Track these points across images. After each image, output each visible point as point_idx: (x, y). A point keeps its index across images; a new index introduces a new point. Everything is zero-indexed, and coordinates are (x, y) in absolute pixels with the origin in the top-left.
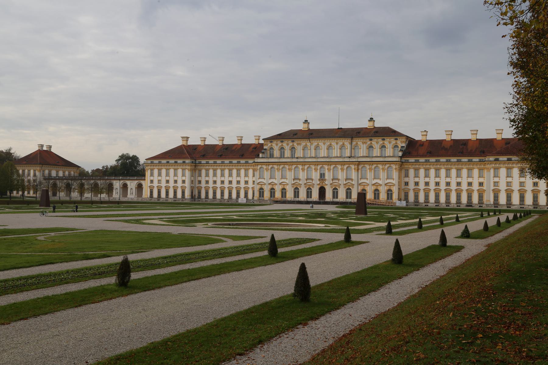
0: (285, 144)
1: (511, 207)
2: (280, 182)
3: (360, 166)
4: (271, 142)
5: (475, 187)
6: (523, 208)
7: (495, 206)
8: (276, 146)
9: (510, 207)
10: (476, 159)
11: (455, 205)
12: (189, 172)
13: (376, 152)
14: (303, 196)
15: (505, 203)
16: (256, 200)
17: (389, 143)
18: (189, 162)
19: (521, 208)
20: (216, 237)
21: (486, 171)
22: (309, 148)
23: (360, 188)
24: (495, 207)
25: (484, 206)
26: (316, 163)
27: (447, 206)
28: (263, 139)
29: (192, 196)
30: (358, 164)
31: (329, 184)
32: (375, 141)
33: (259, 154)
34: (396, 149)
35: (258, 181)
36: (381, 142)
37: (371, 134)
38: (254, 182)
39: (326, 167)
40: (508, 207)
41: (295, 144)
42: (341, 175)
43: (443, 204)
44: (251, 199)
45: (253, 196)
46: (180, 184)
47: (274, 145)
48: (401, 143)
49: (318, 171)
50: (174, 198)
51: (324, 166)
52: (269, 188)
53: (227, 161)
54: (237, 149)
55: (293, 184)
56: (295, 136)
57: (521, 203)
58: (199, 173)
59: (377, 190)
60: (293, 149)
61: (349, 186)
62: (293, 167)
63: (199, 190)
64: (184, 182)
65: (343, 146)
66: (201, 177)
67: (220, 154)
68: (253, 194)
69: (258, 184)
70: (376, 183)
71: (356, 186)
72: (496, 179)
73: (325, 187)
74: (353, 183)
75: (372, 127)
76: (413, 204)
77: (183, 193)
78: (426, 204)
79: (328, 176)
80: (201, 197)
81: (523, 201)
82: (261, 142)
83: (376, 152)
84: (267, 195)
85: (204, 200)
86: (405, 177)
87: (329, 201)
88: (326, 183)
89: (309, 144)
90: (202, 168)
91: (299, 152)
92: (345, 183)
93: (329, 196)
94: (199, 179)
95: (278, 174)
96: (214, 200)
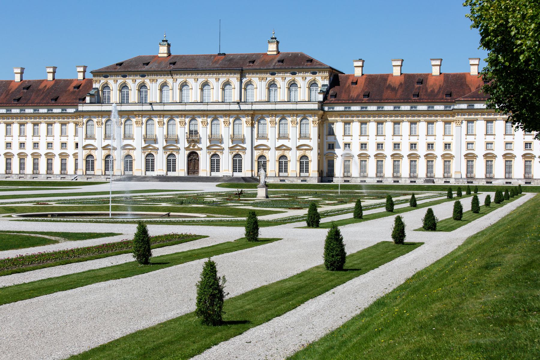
1: (493, 183)
3: (255, 117)
5: (439, 150)
6: (510, 183)
7: (469, 180)
8: (114, 84)
9: (491, 183)
11: (407, 180)
14: (160, 168)
15: (484, 177)
16: (80, 175)
19: (507, 183)
20: (40, 236)
21: (453, 125)
22: (170, 88)
23: (257, 153)
24: (468, 182)
26: (183, 114)
27: (395, 182)
28: (91, 72)
31: (204, 149)
32: (279, 77)
33: (85, 98)
34: (314, 88)
35: (84, 144)
36: (289, 77)
37: (273, 64)
38: (77, 144)
40: (487, 183)
43: (388, 179)
44: (73, 173)
45: (76, 169)
48: (322, 80)
49: (187, 126)
52: (103, 154)
54: (47, 88)
56: (146, 68)
57: (507, 176)
59: (283, 157)
61: (237, 151)
65: (227, 84)
67: (18, 97)
68: (76, 165)
69: (84, 148)
70: (283, 145)
71: (249, 151)
72: (470, 139)
73: (198, 152)
75: (275, 53)
76: (340, 179)
81: (510, 172)
82: (89, 76)
83: (281, 94)
88: (200, 146)
92: (231, 145)
96: (7, 176)
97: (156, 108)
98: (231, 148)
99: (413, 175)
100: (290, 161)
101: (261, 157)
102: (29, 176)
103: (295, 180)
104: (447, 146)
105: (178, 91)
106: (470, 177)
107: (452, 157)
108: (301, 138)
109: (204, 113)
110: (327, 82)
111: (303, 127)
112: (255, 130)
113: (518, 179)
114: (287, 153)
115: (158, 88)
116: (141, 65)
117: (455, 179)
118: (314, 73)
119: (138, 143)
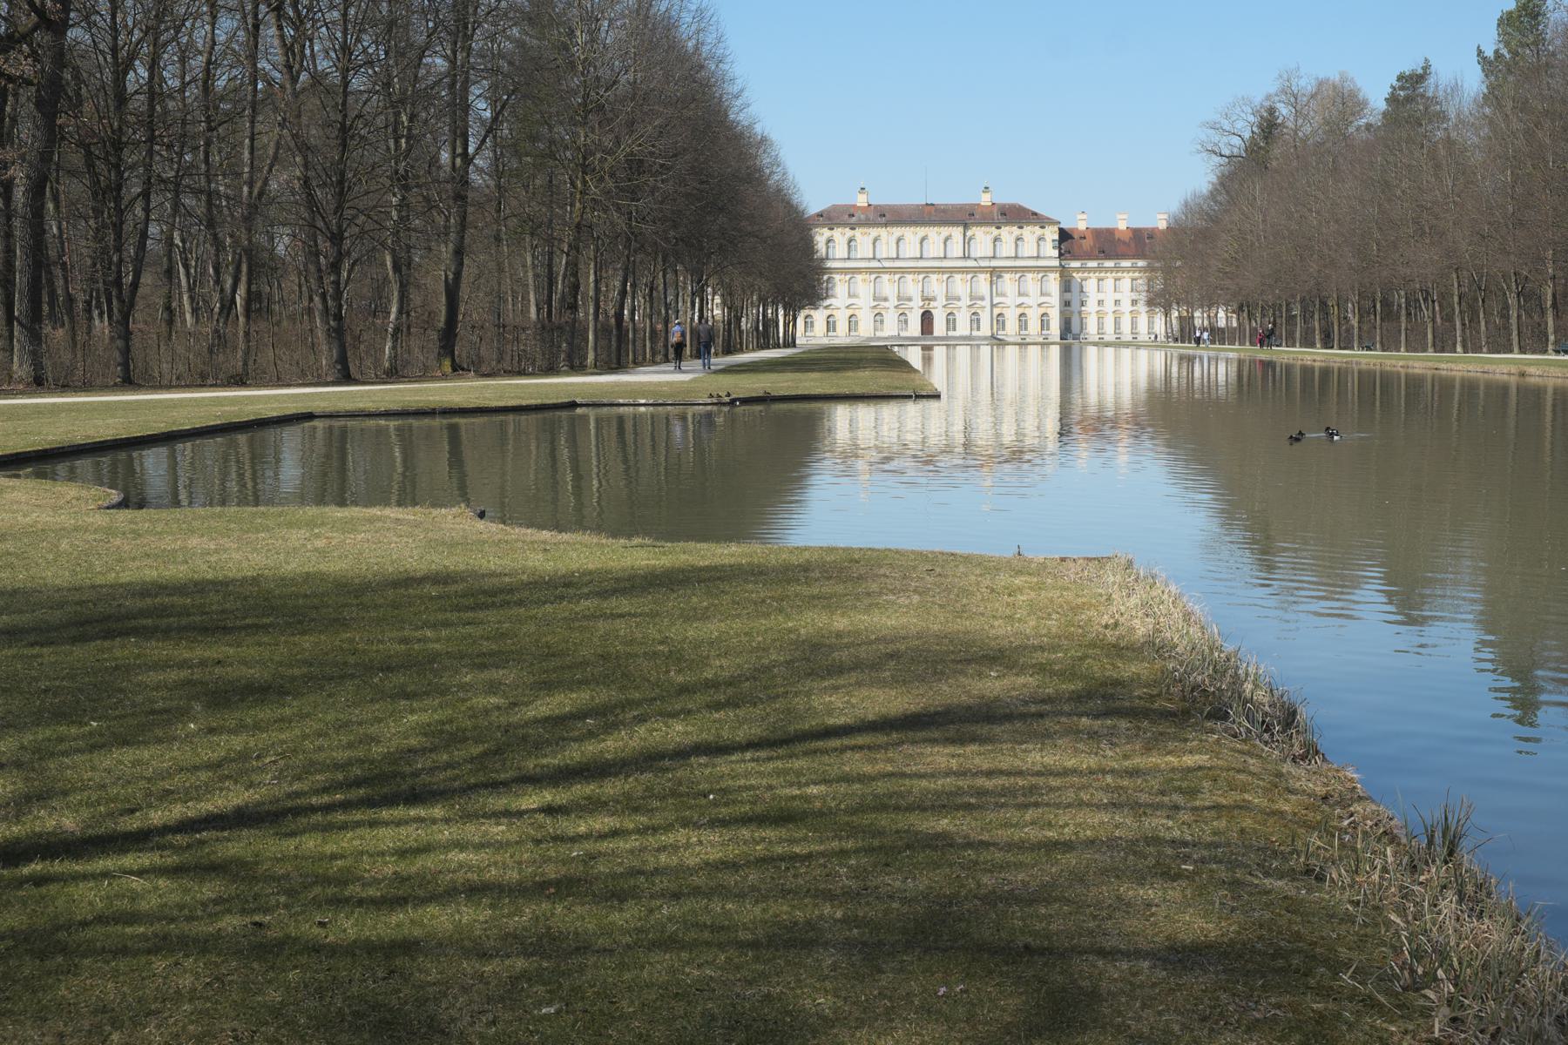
13: (1007, 249)
17: (1030, 233)
23: (996, 311)
48: (1051, 234)
55: (875, 307)
73: (932, 311)
86: (1066, 291)
92: (969, 303)
97: (887, 264)
98: (970, 306)
101: (999, 315)
105: (894, 246)
108: (1042, 294)
110: (1056, 237)
111: (1044, 283)
112: (994, 286)
114: (1027, 311)
115: (871, 242)
118: (1042, 227)
119: (864, 301)
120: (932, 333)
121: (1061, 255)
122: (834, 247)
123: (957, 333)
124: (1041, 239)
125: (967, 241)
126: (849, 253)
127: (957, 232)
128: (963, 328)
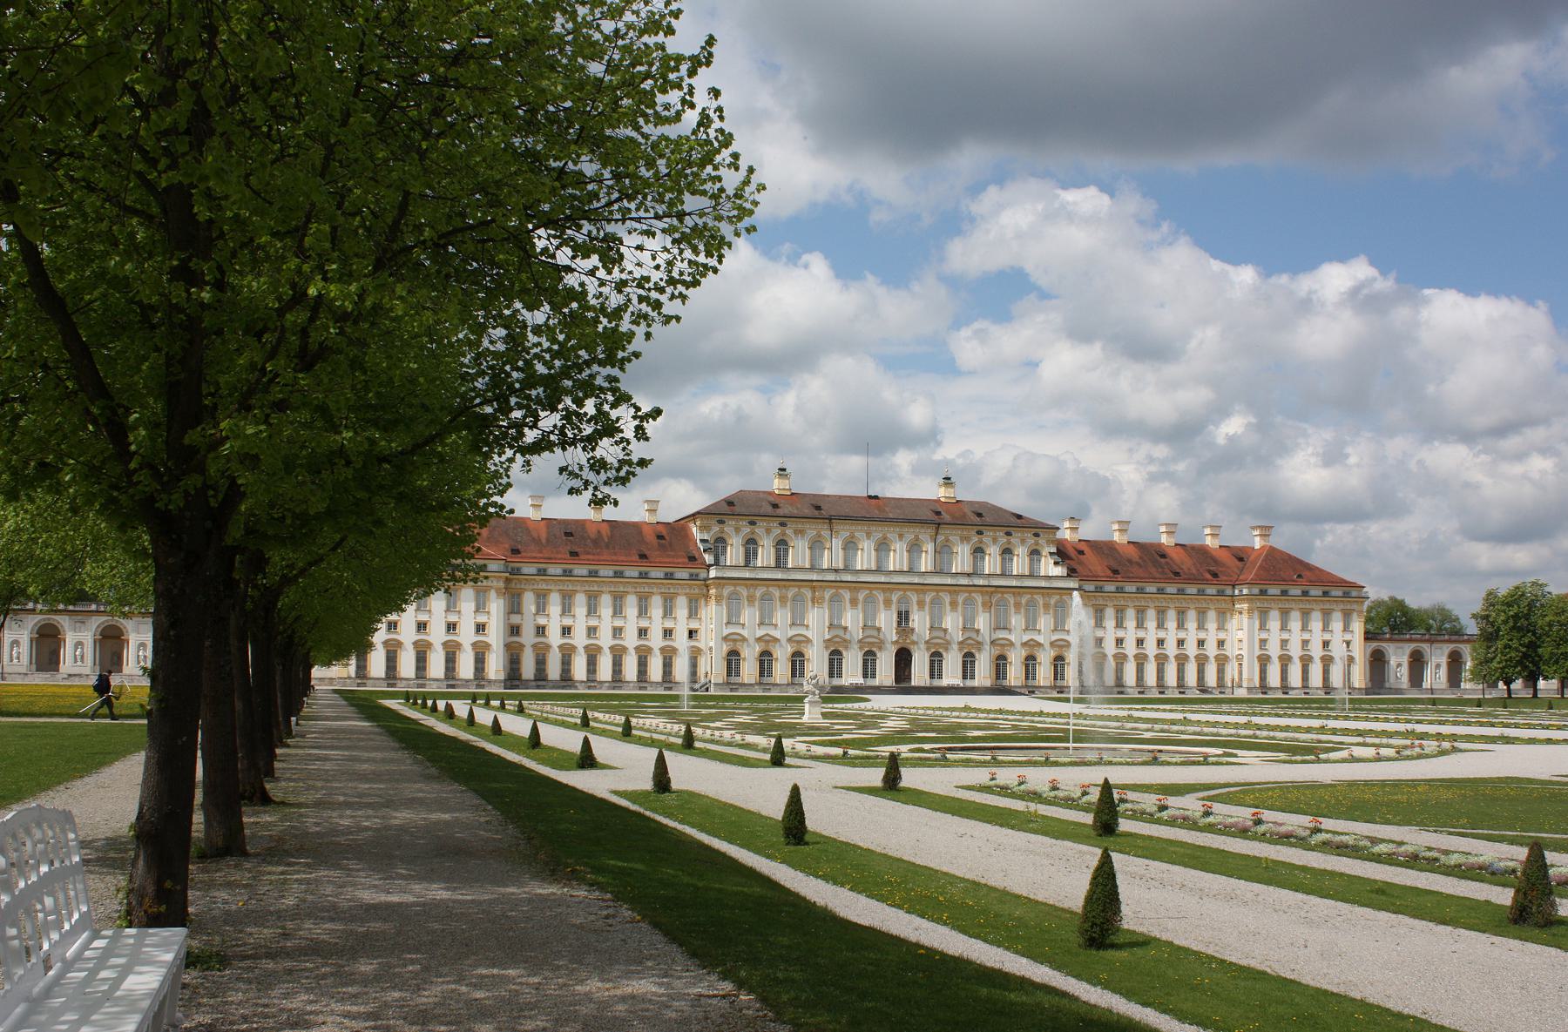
0: (759, 531)
2: (789, 636)
4: (721, 522)
5: (1211, 650)
6: (1307, 693)
10: (1211, 590)
12: (501, 602)
13: (991, 564)
18: (502, 568)
25: (1227, 691)
26: (888, 587)
29: (513, 676)
30: (992, 593)
39: (914, 598)
41: (789, 532)
42: (952, 622)
43: (1154, 690)
46: (467, 635)
47: (728, 529)
50: (447, 677)
51: (909, 593)
53: (606, 571)
56: (780, 512)
58: (513, 602)
60: (781, 546)
62: (827, 595)
63: (512, 655)
64: (480, 628)
66: (522, 614)
69: (725, 639)
70: (1032, 640)
74: (980, 639)
77: (480, 661)
78: (1119, 689)
79: (919, 622)
80: (521, 675)
84: (749, 671)
85: (534, 683)
87: (923, 685)
88: (914, 638)
89: (826, 533)
90: (523, 586)
91: (799, 554)
92: (961, 639)
93: (919, 673)
94: (515, 619)
95: (782, 616)
99: (1181, 684)
100: (1011, 663)
102: (607, 684)
103: (1049, 691)
104: (1221, 643)
106: (1264, 688)
107: (1226, 658)
109: (922, 588)
110: (1054, 550)
113: (1317, 689)
116: (769, 510)
117: (1248, 688)
118: (1037, 535)
120: (909, 678)
121: (1069, 576)
122: (755, 554)
123: (976, 683)
124: (1035, 553)
125: (943, 551)
126: (778, 559)
127: (925, 535)
128: (951, 675)
